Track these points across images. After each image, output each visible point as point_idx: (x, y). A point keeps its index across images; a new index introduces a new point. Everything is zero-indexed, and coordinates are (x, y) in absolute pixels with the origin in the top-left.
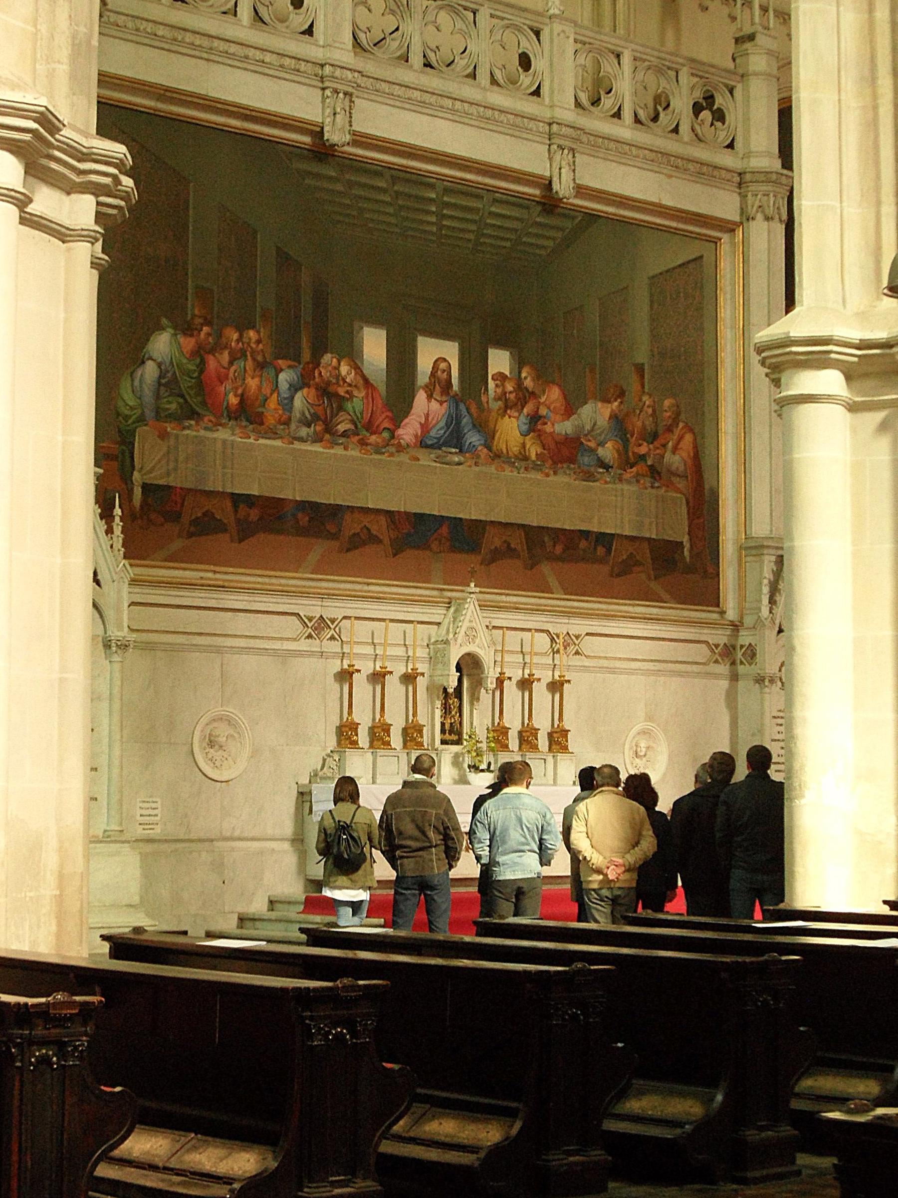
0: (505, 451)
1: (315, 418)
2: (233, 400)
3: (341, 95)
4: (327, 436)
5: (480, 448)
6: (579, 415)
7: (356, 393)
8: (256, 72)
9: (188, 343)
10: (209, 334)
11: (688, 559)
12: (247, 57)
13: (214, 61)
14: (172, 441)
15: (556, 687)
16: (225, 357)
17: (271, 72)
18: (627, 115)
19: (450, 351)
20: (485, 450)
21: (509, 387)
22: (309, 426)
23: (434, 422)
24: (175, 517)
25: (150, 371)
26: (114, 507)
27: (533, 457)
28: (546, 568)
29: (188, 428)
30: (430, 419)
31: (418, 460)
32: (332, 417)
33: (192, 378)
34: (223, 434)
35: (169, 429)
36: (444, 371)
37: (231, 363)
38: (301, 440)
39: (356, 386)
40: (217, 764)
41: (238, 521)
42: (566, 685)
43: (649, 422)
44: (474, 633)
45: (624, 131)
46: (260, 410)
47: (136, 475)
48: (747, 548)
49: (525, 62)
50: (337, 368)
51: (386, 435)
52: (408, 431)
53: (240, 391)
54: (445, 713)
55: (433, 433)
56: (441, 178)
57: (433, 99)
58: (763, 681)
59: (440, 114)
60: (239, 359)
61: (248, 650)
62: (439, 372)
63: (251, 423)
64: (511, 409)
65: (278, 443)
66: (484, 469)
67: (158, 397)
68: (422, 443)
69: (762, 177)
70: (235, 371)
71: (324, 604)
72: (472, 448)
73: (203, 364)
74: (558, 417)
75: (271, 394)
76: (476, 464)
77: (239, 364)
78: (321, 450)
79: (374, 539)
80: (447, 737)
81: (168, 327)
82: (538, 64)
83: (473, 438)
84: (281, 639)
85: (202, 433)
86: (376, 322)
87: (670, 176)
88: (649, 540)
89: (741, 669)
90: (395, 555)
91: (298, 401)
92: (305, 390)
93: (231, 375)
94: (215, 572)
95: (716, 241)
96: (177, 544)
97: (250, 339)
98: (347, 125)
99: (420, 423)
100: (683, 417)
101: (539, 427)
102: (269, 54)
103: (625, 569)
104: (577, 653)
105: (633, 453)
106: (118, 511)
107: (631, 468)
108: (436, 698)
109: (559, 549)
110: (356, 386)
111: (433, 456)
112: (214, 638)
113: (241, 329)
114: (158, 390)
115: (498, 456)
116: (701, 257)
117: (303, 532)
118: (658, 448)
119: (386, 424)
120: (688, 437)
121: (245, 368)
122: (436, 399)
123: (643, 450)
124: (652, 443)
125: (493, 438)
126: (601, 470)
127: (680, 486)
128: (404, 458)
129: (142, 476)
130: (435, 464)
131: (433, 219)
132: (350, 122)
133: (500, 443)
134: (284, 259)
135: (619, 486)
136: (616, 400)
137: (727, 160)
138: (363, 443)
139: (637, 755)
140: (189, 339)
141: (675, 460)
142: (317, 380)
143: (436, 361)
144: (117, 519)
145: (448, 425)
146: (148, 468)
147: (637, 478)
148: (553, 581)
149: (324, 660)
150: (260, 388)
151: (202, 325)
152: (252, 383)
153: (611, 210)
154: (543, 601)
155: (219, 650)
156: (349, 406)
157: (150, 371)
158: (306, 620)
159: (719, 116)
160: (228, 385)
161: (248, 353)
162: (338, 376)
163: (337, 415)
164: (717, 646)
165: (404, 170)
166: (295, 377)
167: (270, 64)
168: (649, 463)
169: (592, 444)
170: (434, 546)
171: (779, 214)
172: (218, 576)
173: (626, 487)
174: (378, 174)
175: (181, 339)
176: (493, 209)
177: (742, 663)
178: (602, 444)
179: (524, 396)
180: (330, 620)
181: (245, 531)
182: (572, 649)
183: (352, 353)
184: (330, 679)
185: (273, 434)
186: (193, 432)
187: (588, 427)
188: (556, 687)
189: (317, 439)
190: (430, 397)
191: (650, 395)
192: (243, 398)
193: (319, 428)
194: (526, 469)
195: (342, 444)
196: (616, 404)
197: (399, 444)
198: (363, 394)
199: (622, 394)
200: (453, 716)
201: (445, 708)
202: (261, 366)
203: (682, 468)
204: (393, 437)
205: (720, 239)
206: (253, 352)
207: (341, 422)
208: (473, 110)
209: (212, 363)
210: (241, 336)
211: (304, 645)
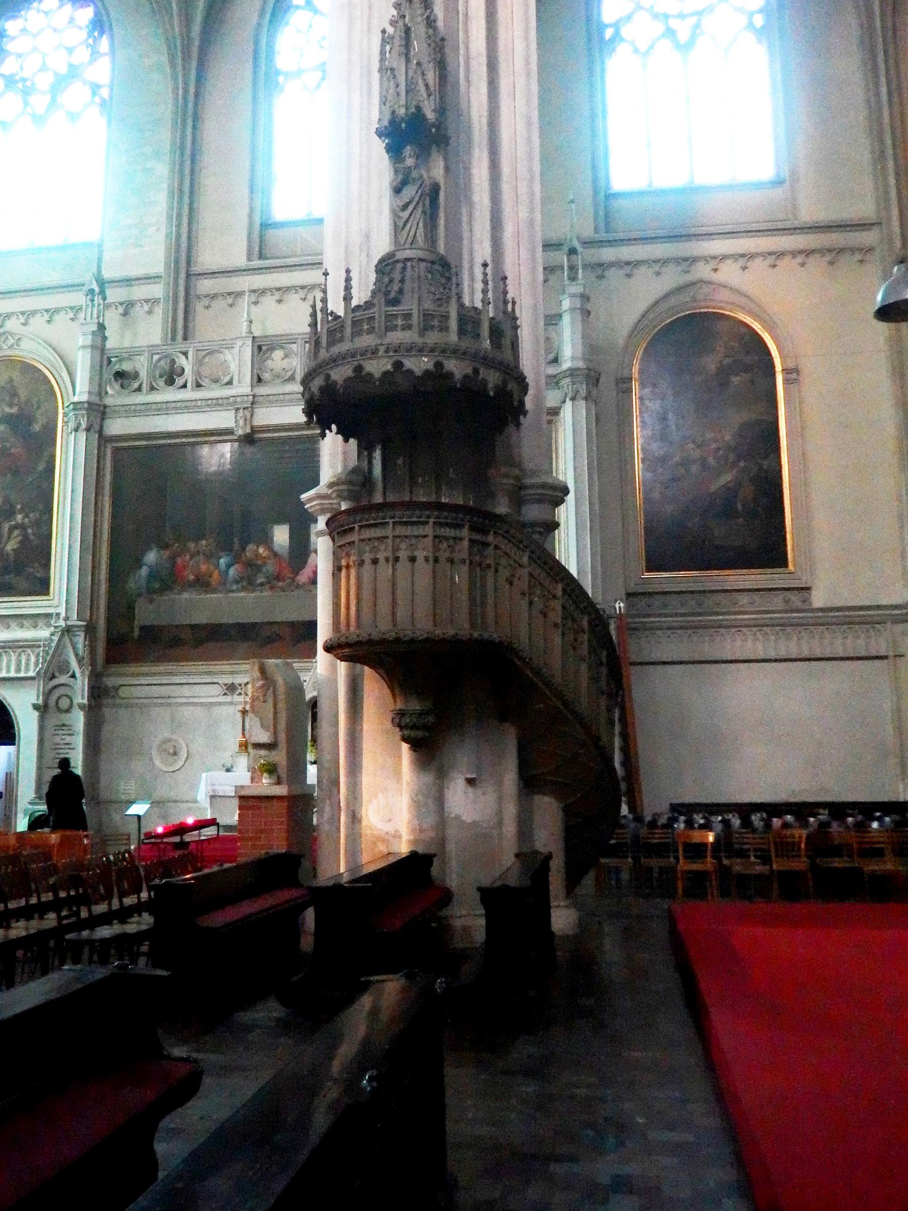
1: (242, 579)
2: (192, 577)
4: (250, 587)
9: (166, 554)
10: (178, 547)
25: (144, 571)
34: (185, 595)
37: (191, 559)
38: (233, 591)
47: (136, 623)
65: (220, 595)
73: (175, 562)
79: (279, 638)
92: (236, 566)
128: (301, 591)
138: (272, 588)
151: (174, 543)
155: (169, 705)
156: (264, 570)
157: (144, 571)
175: (162, 552)
181: (199, 643)
185: (214, 591)
189: (243, 589)
204: (293, 580)
209: (179, 560)
211: (222, 699)
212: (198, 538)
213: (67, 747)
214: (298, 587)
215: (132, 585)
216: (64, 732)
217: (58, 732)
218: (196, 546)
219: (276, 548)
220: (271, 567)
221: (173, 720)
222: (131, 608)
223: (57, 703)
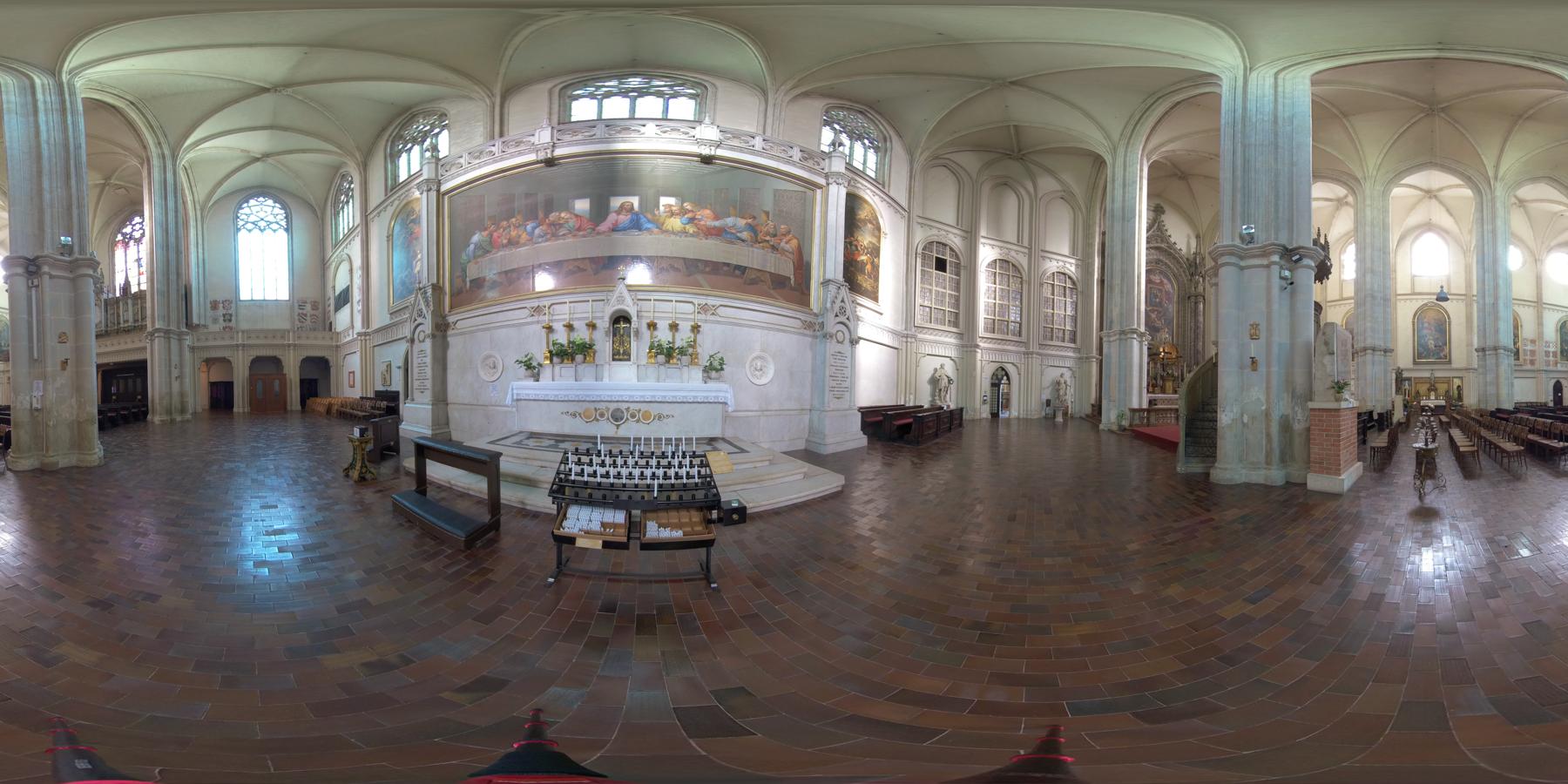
1: (546, 234)
65: (526, 248)
104: (713, 314)
123: (768, 238)
135: (751, 249)
169: (734, 231)
173: (755, 250)
220: (572, 223)
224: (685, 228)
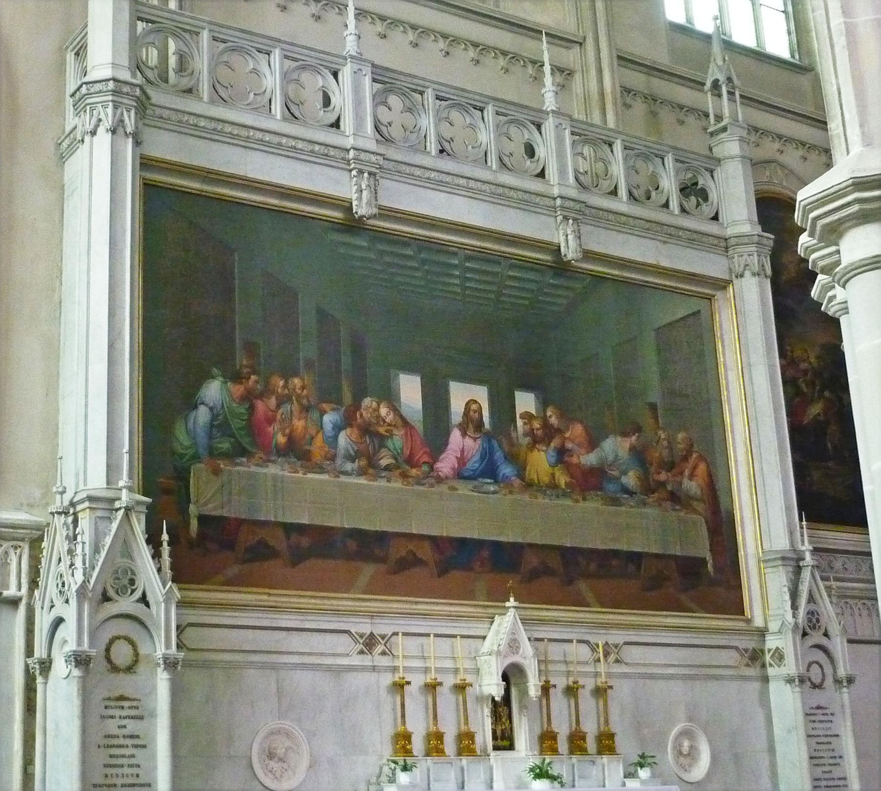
0: (536, 481)
2: (281, 439)
3: (366, 175)
4: (371, 471)
5: (513, 478)
6: (601, 448)
7: (395, 432)
8: (289, 157)
9: (238, 390)
10: (257, 382)
11: (712, 574)
12: (280, 144)
13: (251, 148)
14: (225, 478)
15: (600, 692)
16: (273, 402)
17: (302, 157)
18: (623, 192)
19: (481, 394)
20: (518, 481)
21: (536, 425)
22: (353, 462)
23: (470, 456)
24: (229, 545)
25: (202, 415)
26: (162, 533)
27: (563, 487)
28: (582, 586)
29: (240, 464)
30: (465, 454)
31: (457, 490)
32: (374, 455)
33: (243, 420)
34: (273, 470)
35: (222, 466)
36: (475, 411)
37: (278, 406)
38: (345, 473)
39: (395, 426)
40: (278, 775)
41: (290, 547)
42: (609, 691)
43: (665, 453)
44: (517, 645)
45: (621, 204)
46: (307, 447)
47: (192, 508)
48: (765, 561)
49: (530, 151)
50: (377, 410)
51: (425, 468)
52: (446, 464)
53: (287, 431)
54: (496, 718)
55: (469, 465)
56: (462, 247)
57: (448, 179)
58: (794, 681)
59: (457, 192)
60: (286, 402)
61: (304, 666)
62: (472, 413)
63: (299, 460)
64: (539, 442)
65: (325, 477)
66: (518, 497)
67: (210, 437)
68: (460, 475)
69: (746, 240)
70: (282, 414)
71: (374, 621)
72: (506, 478)
73: (252, 409)
74: (583, 451)
75: (317, 434)
76: (511, 492)
77: (286, 408)
78: (365, 482)
80: (500, 743)
81: (218, 376)
82: (541, 152)
83: (506, 470)
84: (334, 655)
85: (253, 469)
86: (410, 369)
87: (665, 242)
88: (675, 557)
89: (771, 671)
90: (439, 576)
91: (343, 439)
92: (349, 430)
93: (279, 417)
94: (269, 594)
95: (710, 298)
96: (234, 570)
97: (295, 386)
98: (373, 199)
99: (457, 457)
100: (696, 448)
101: (566, 459)
102: (300, 142)
103: (657, 582)
105: (654, 480)
106: (165, 537)
107: (653, 493)
108: (485, 706)
109: (593, 567)
110: (395, 426)
111: (470, 487)
112: (270, 656)
113: (286, 377)
114: (211, 431)
115: (529, 485)
116: (699, 312)
117: (350, 557)
118: (675, 476)
119: (425, 459)
120: (702, 467)
121: (291, 411)
122: (469, 436)
123: (663, 476)
124: (669, 471)
125: (525, 469)
126: (625, 496)
127: (698, 508)
128: (444, 488)
129: (197, 507)
130: (473, 493)
131: (457, 281)
132: (376, 197)
133: (531, 474)
134: (322, 315)
136: (634, 434)
137: (712, 228)
138: (404, 476)
139: (680, 753)
140: (238, 387)
141: (692, 486)
142: (359, 421)
143: (467, 404)
144: (165, 544)
145: (482, 458)
146: (202, 501)
147: (659, 503)
148: (589, 596)
149: (376, 674)
150: (306, 428)
151: (250, 374)
152: (299, 424)
153: (616, 272)
154: (581, 615)
155: (274, 667)
156: (389, 443)
157: (202, 415)
158: (357, 637)
159: (703, 195)
160: (276, 426)
161: (294, 398)
162: (378, 417)
163: (379, 450)
164: (746, 650)
165: (429, 241)
166: (339, 421)
167: (301, 150)
168: (669, 488)
169: (615, 473)
170: (477, 566)
171: (764, 270)
172: (272, 598)
174: (406, 244)
176: (511, 273)
177: (771, 665)
178: (625, 473)
179: (549, 433)
180: (380, 636)
181: (297, 557)
182: (612, 658)
183: (390, 396)
184: (383, 694)
185: (321, 470)
186: (245, 468)
187: (611, 458)
188: (600, 692)
189: (362, 472)
190: (464, 434)
191: (664, 429)
192: (290, 439)
193: (363, 462)
194: (558, 497)
195: (384, 477)
196: (634, 438)
197: (439, 477)
198: (402, 432)
199: (638, 429)
200: (504, 723)
201: (495, 715)
202: (306, 409)
203: (699, 492)
204: (432, 469)
205: (714, 296)
206: (299, 397)
207: (381, 458)
208: (485, 187)
209: (260, 405)
210: (286, 382)
211: (357, 660)
212: (288, 374)
213: (129, 742)
214: (440, 480)
215: (182, 436)
216: (124, 713)
217: (111, 712)
218: (285, 386)
219: (405, 411)
221: (280, 692)
222: (182, 476)
223: (108, 650)
224: (553, 475)
